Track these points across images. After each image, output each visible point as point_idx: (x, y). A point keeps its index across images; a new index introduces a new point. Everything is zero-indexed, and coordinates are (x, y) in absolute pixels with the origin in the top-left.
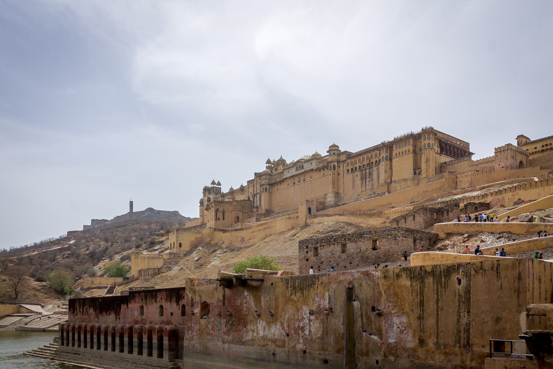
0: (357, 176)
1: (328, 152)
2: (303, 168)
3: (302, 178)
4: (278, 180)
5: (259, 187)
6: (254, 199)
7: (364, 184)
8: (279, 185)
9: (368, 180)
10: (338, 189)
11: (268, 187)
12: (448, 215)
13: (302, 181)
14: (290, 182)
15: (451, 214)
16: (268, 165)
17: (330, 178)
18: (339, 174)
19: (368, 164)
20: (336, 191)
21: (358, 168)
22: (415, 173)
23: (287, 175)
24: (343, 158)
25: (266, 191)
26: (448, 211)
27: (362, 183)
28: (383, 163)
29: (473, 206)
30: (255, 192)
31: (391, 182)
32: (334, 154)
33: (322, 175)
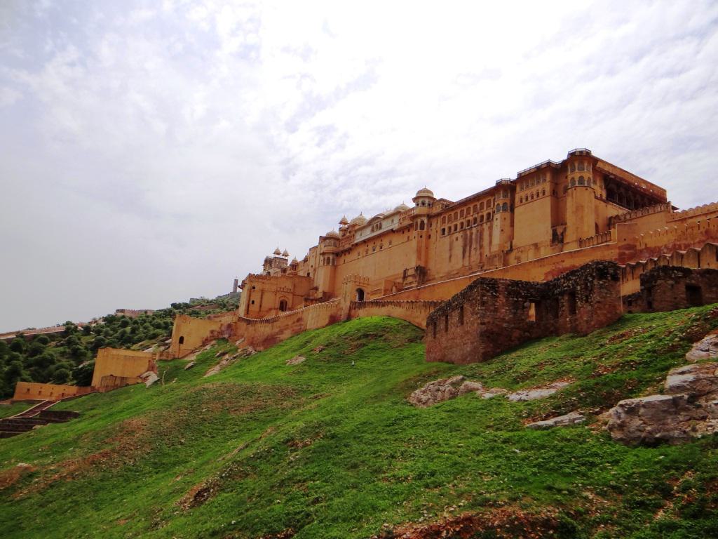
0: (457, 239)
1: (415, 200)
2: (380, 228)
3: (378, 243)
4: (347, 246)
6: (314, 274)
7: (467, 254)
9: (474, 246)
10: (426, 262)
11: (331, 258)
12: (573, 310)
13: (378, 249)
14: (361, 249)
15: (584, 310)
16: (342, 226)
17: (414, 243)
18: (429, 237)
20: (423, 265)
21: (459, 227)
22: (555, 234)
23: (359, 238)
24: (437, 209)
25: (328, 263)
26: (572, 294)
28: (497, 216)
29: (677, 280)
31: (511, 249)
32: (423, 204)
33: (406, 239)
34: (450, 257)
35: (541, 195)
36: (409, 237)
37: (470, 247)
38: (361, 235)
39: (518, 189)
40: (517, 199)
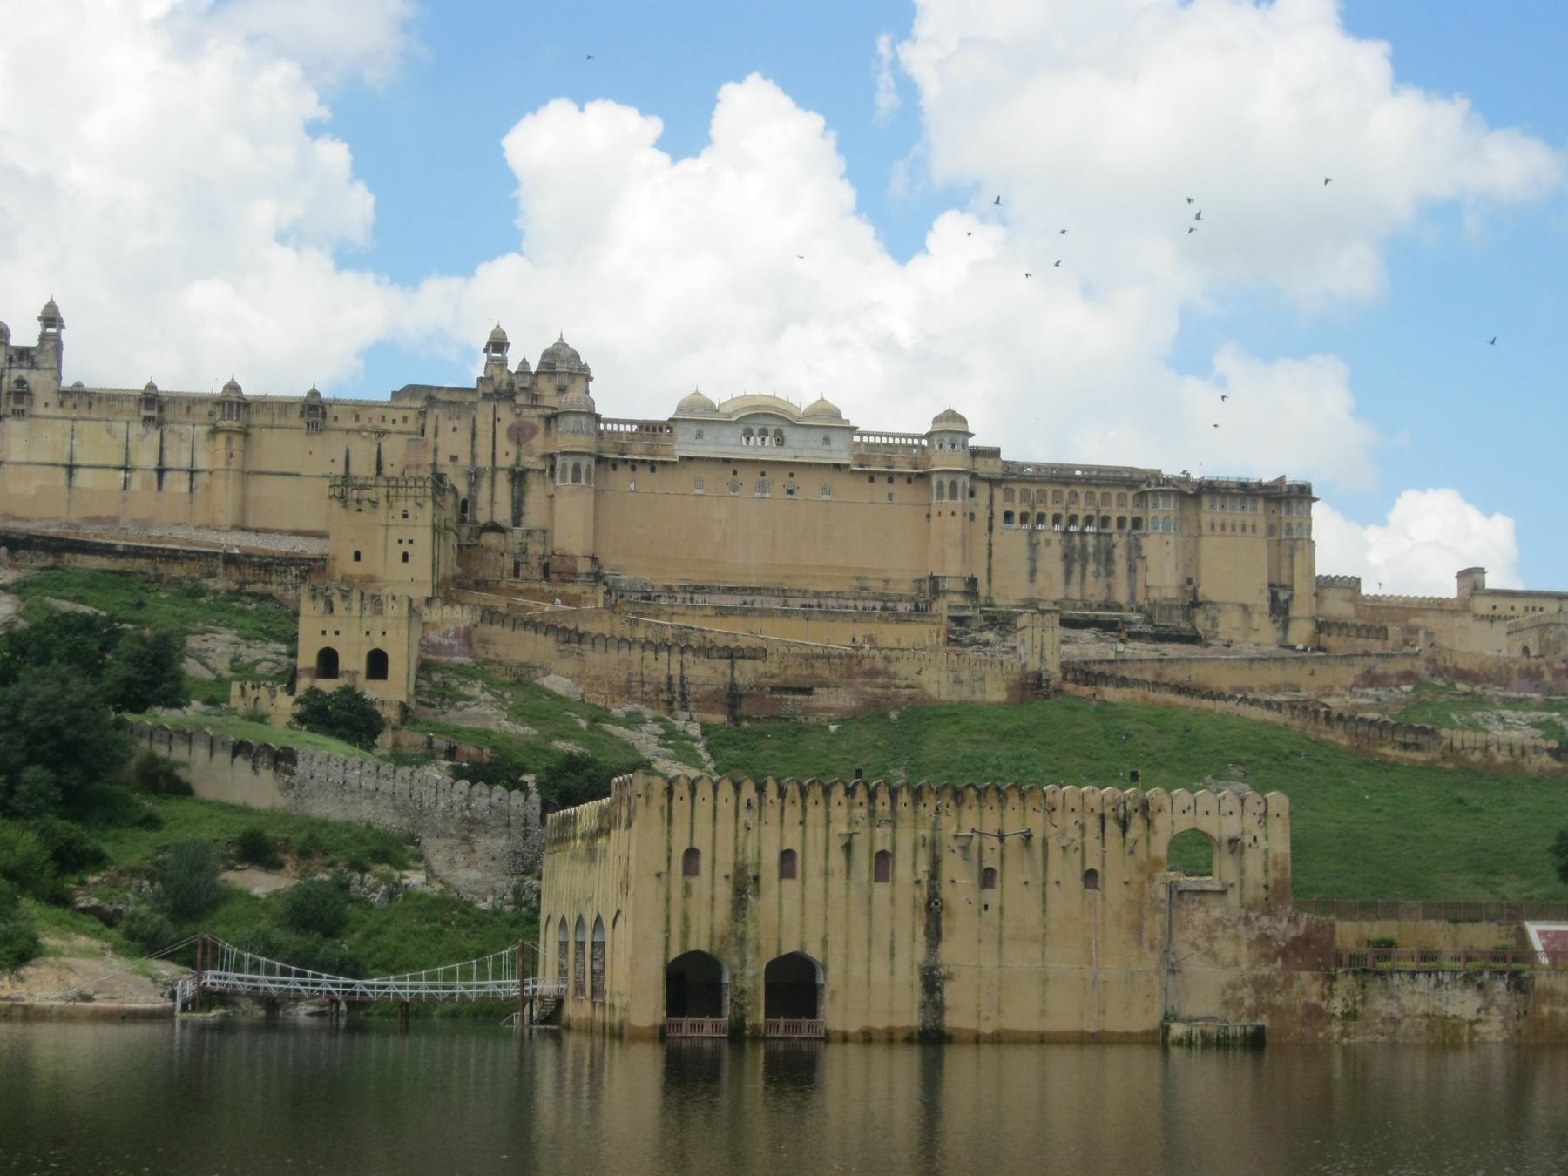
0: (1048, 543)
2: (781, 441)
3: (779, 479)
5: (504, 444)
7: (1076, 577)
8: (643, 472)
9: (1091, 567)
18: (972, 517)
19: (1089, 520)
22: (1274, 598)
25: (588, 479)
27: (1068, 573)
30: (484, 461)
34: (1033, 572)
35: (1249, 530)
36: (890, 496)
37: (1084, 567)
38: (699, 436)
39: (1206, 501)
40: (1206, 519)
